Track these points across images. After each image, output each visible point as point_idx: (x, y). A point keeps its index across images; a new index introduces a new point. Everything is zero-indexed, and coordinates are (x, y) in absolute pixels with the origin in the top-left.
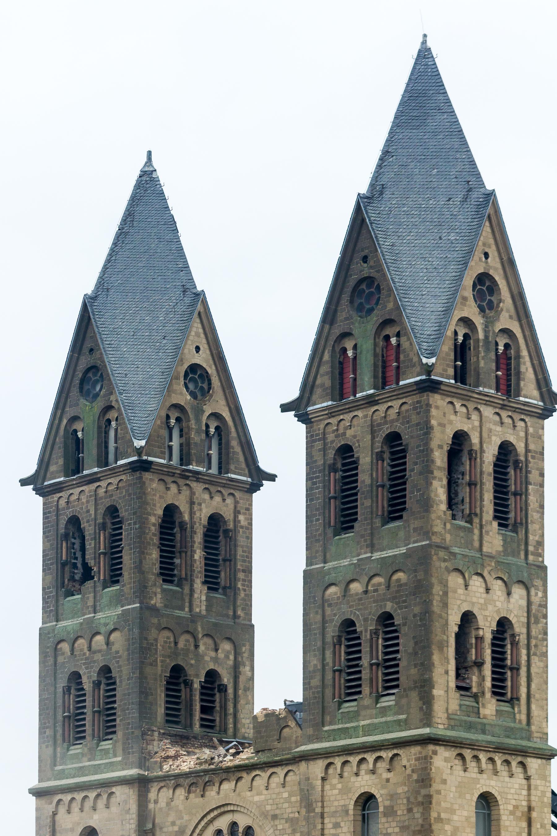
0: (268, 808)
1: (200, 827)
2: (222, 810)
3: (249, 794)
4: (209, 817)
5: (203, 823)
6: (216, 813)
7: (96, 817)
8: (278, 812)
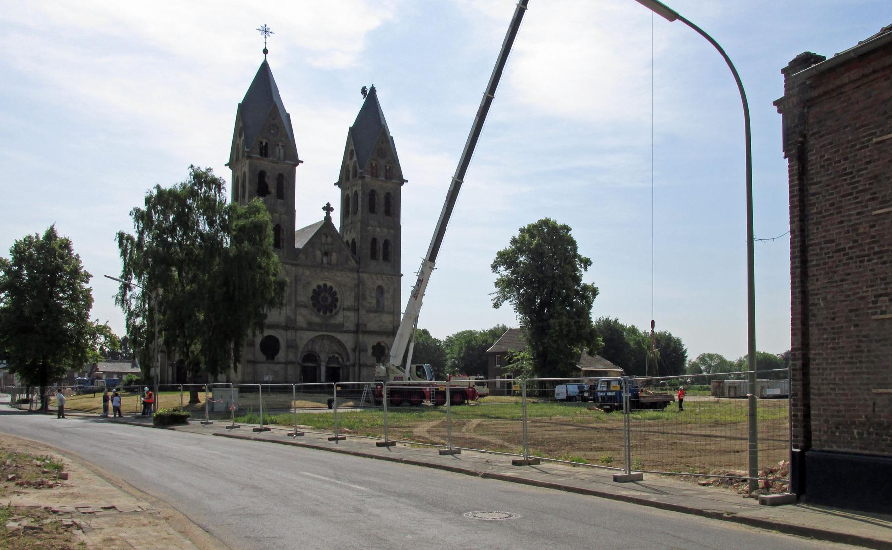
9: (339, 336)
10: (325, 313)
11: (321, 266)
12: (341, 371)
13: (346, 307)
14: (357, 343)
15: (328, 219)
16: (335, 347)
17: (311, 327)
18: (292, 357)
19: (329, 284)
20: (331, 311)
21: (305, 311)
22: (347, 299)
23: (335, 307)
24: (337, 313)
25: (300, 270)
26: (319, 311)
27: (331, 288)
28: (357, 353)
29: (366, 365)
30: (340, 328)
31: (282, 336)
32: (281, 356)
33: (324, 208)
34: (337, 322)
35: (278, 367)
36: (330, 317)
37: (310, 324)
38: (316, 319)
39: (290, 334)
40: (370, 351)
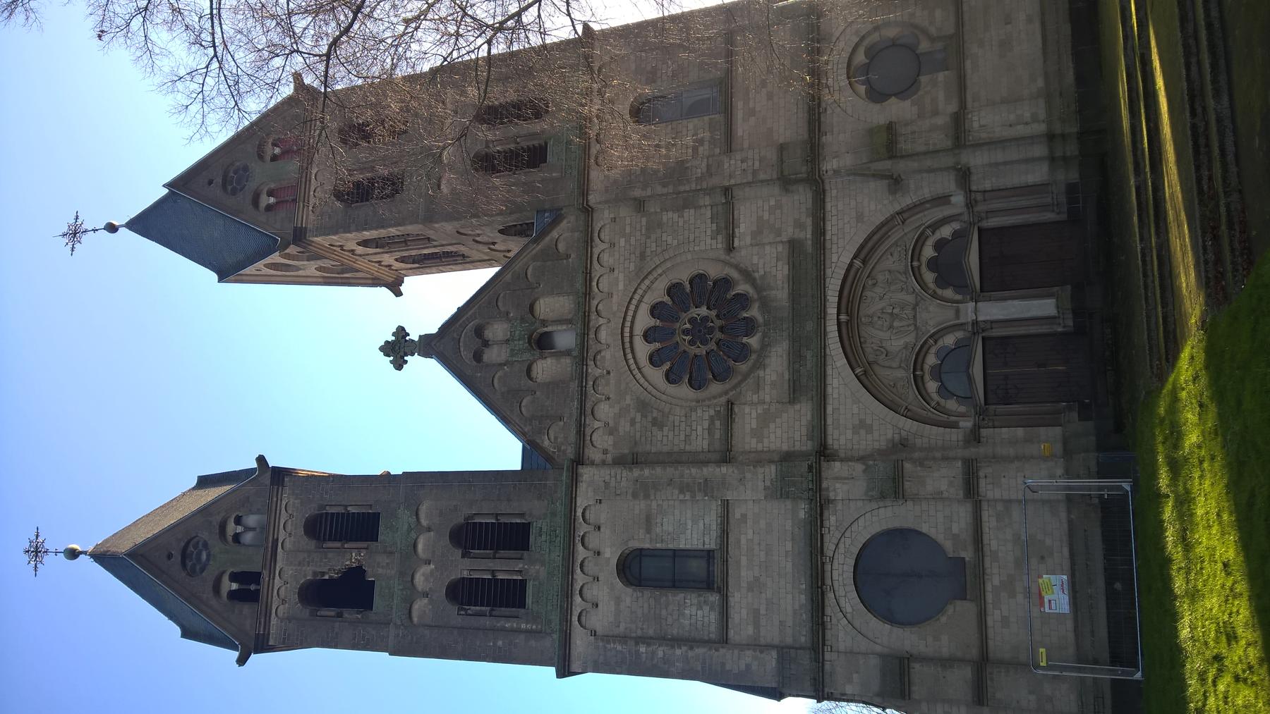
0: (632, 267)
1: (642, 381)
2: (627, 345)
3: (615, 297)
4: (633, 367)
5: (639, 376)
6: (630, 356)
7: (607, 553)
8: (638, 253)
9: (840, 257)
10: (750, 327)
11: (583, 355)
12: (993, 222)
13: (720, 244)
14: (860, 173)
15: (428, 346)
16: (891, 262)
17: (808, 385)
18: (944, 478)
19: (644, 320)
20: (743, 300)
21: (747, 418)
23: (726, 283)
24: (747, 275)
26: (744, 352)
27: (655, 310)
28: (901, 166)
29: (959, 119)
30: (807, 258)
31: (857, 520)
32: (940, 519)
33: (399, 365)
34: (781, 272)
35: (999, 541)
36: (765, 304)
37: (795, 392)
38: (776, 365)
39: (844, 484)
40: (897, 109)
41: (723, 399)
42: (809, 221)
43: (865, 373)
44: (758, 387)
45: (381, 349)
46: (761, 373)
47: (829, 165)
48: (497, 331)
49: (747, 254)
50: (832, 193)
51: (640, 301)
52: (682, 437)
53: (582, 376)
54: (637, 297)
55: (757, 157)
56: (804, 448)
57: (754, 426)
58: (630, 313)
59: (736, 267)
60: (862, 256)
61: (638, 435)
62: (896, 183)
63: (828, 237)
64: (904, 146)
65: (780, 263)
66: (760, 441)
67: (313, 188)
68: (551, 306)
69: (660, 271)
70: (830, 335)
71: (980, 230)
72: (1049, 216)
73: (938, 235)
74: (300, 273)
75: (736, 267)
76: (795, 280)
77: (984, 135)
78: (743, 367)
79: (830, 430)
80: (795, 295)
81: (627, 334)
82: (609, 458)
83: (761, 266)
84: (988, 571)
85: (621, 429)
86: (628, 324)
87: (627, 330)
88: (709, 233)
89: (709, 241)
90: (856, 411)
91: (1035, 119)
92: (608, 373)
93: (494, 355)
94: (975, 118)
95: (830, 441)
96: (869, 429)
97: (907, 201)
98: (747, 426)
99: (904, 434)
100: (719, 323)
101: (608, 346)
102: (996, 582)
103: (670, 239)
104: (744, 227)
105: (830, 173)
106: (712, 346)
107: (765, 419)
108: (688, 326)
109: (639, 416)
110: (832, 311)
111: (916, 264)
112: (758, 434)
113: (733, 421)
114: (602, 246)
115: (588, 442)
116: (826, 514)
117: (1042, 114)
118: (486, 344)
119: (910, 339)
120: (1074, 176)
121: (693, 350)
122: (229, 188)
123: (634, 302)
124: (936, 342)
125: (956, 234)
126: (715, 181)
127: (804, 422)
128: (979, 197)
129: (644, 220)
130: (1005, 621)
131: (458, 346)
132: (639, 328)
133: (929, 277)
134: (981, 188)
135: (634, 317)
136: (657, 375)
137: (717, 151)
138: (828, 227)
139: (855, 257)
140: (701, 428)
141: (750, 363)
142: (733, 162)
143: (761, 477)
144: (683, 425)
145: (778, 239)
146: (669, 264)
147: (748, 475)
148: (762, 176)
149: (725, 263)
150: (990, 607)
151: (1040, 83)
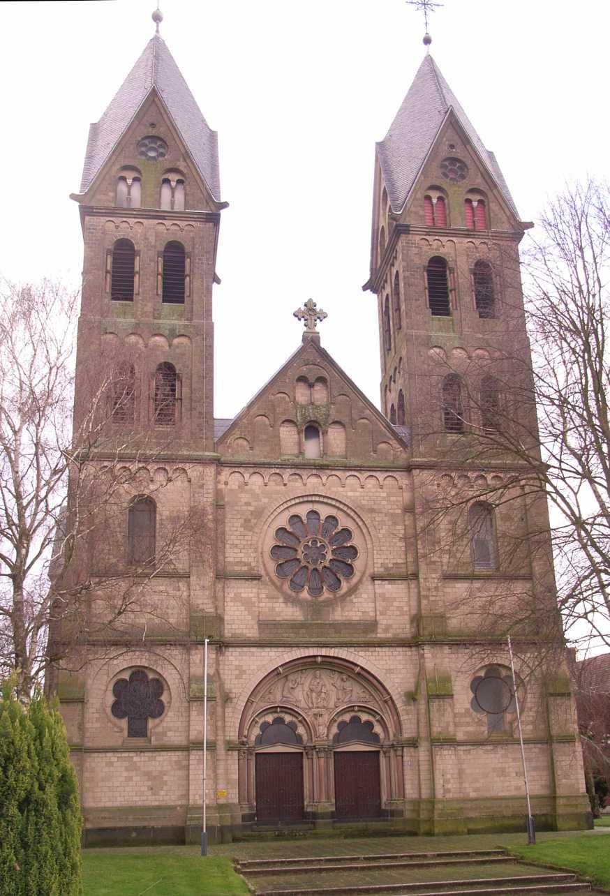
0: (363, 502)
2: (305, 499)
3: (342, 489)
4: (289, 504)
5: (282, 508)
6: (297, 501)
8: (375, 507)
9: (362, 658)
11: (300, 466)
13: (379, 570)
14: (421, 672)
15: (311, 342)
16: (357, 693)
18: (201, 726)
21: (248, 591)
22: (380, 548)
24: (353, 590)
25: (231, 479)
26: (297, 587)
29: (451, 742)
35: (164, 761)
36: (331, 604)
38: (289, 612)
40: (463, 697)
41: (263, 573)
42: (389, 635)
43: (279, 674)
44: (271, 598)
45: (310, 300)
46: (281, 600)
47: (428, 652)
48: (320, 393)
49: (367, 590)
50: (409, 652)
51: (339, 508)
52: (236, 542)
53: (282, 466)
54: (341, 506)
55: (438, 598)
56: (226, 631)
57: (243, 595)
58: (329, 501)
59: (360, 581)
60: (363, 673)
61: (236, 508)
62: (411, 697)
63: (377, 649)
64: (435, 704)
65: (360, 614)
66: (234, 600)
67: (441, 238)
68: (336, 438)
69: (360, 523)
70: (306, 650)
71: (378, 752)
72: (384, 798)
73: (375, 723)
74: (381, 212)
75: (360, 581)
76: (350, 625)
77: (438, 757)
78: (286, 587)
79: (239, 650)
80: (336, 627)
81: (314, 499)
82: (221, 486)
83: (360, 600)
84: (142, 754)
85: (243, 495)
86: (321, 499)
87: (317, 499)
88: (387, 561)
89: (380, 561)
90: (252, 668)
91: (447, 791)
92: (285, 485)
93: (302, 395)
94: (450, 752)
95: (231, 649)
96: (238, 677)
97: (399, 705)
98: (243, 590)
99: (235, 701)
100: (320, 568)
101: (305, 485)
102: (135, 759)
103: (383, 531)
104: (388, 588)
105: (422, 651)
106: (303, 563)
107: (247, 603)
108: (319, 544)
109: (251, 508)
110: (324, 652)
111: (356, 708)
112: (237, 598)
113: (247, 580)
114: (381, 479)
115: (234, 469)
116: (179, 647)
117: (450, 796)
118: (311, 386)
119: (303, 704)
120: (408, 815)
121: (300, 549)
122: (447, 163)
123: (337, 504)
124: (300, 721)
125: (376, 736)
126: (423, 567)
127: (244, 631)
128: (399, 753)
129: (399, 511)
130: (111, 764)
131: (312, 365)
132: (317, 507)
133: (347, 717)
134: (405, 754)
135: (326, 504)
136: (283, 521)
137: (445, 568)
138: (384, 649)
139: (362, 668)
140: (242, 556)
141: (289, 592)
142: (436, 581)
143: (206, 601)
144: (245, 543)
145: (378, 613)
146: (365, 530)
147: (207, 593)
148: (424, 602)
149: (364, 573)
150: (119, 755)
151: (473, 795)
